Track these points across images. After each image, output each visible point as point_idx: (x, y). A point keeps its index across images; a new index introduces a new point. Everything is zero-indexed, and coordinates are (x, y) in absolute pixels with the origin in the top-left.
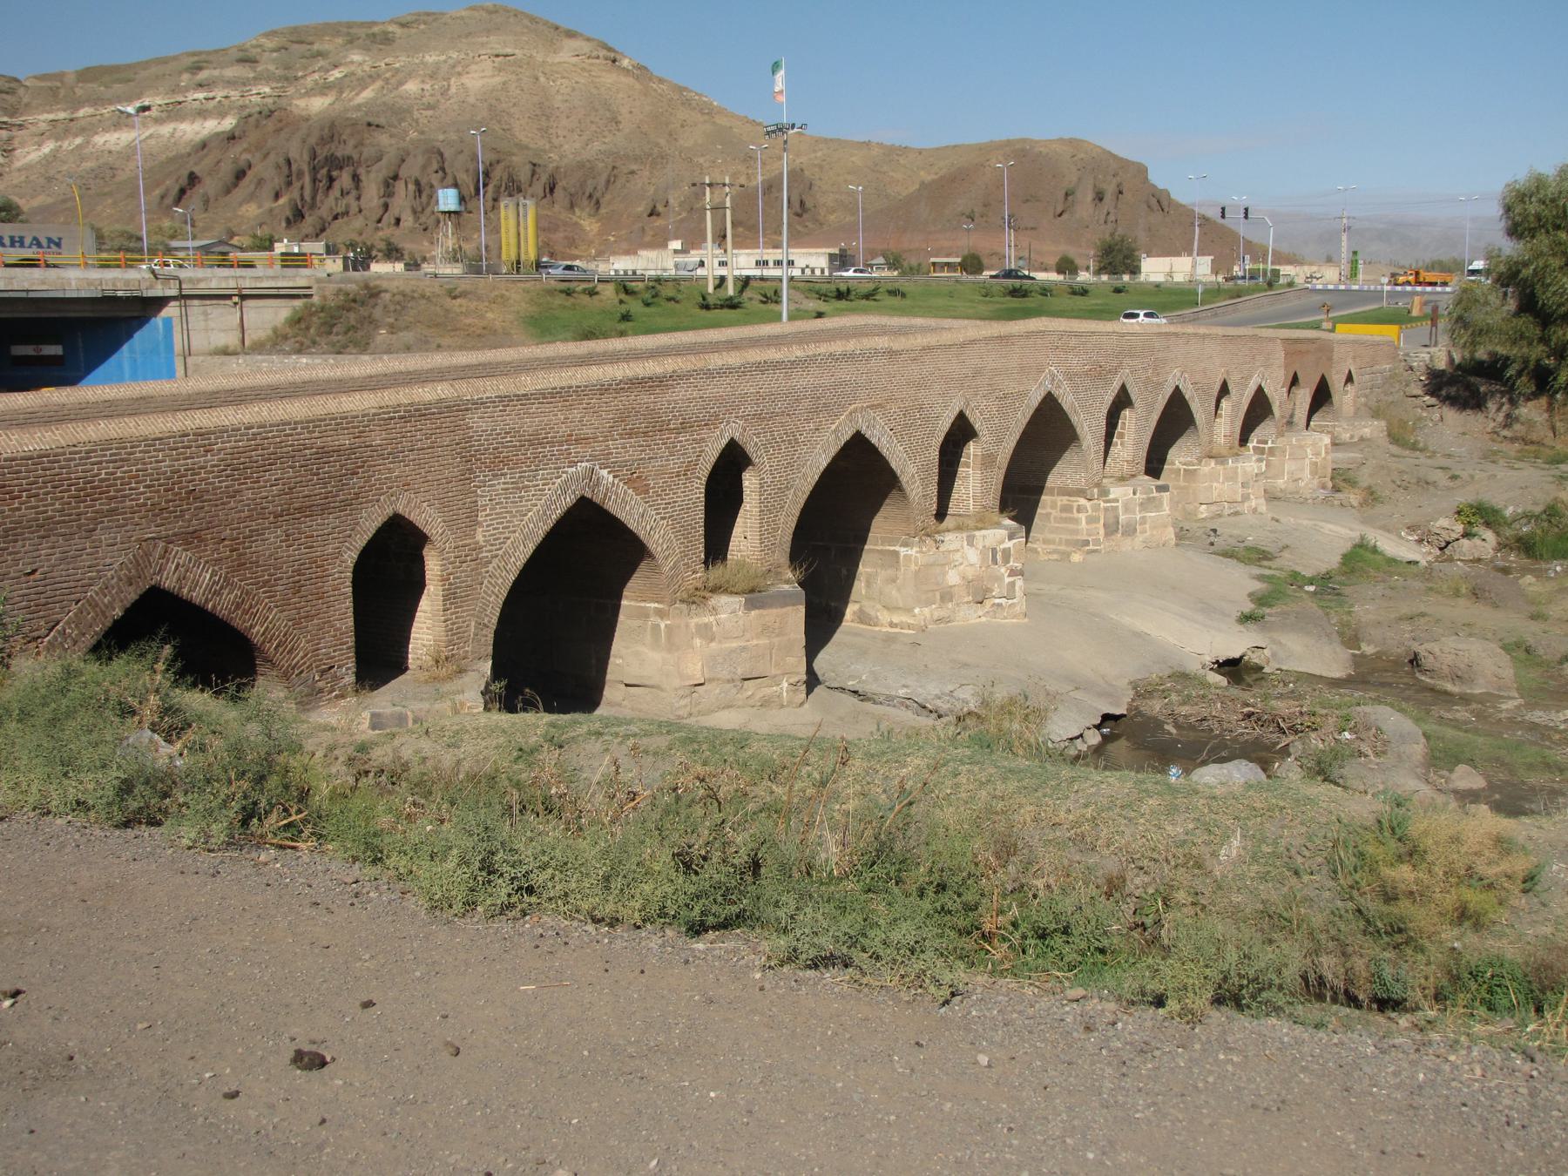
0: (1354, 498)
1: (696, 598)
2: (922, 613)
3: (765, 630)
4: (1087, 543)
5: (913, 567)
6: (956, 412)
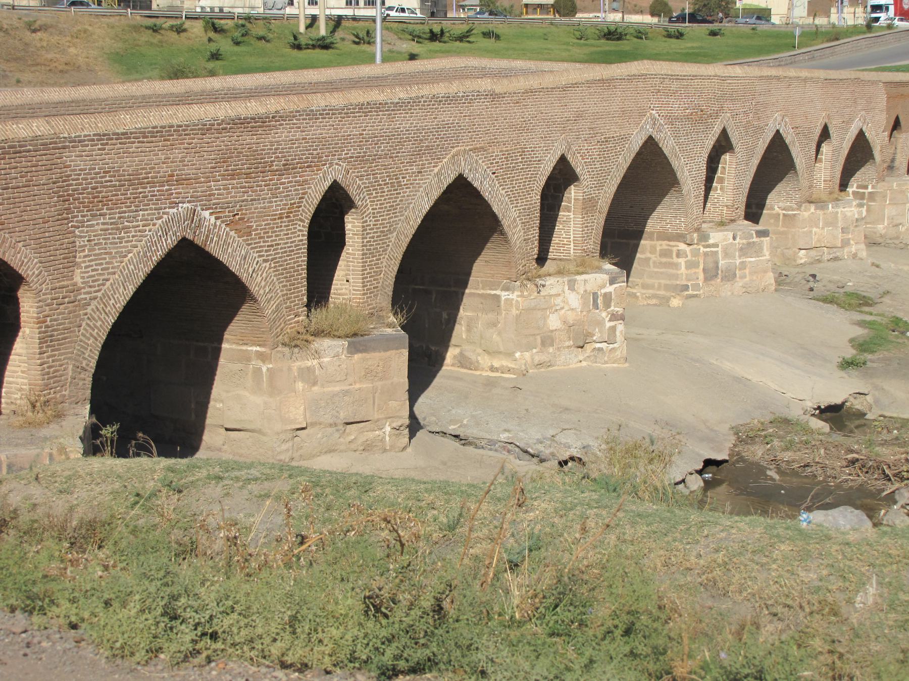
1: (297, 342)
2: (523, 357)
3: (369, 374)
4: (686, 288)
5: (514, 312)
6: (557, 157)
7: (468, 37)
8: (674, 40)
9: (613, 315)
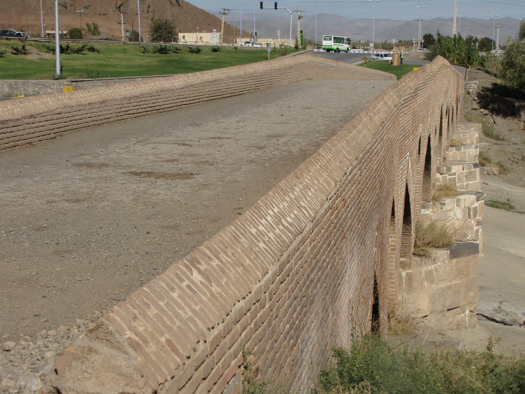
0: (496, 170)
3: (460, 273)
7: (82, 51)
8: (195, 54)
9: (478, 221)
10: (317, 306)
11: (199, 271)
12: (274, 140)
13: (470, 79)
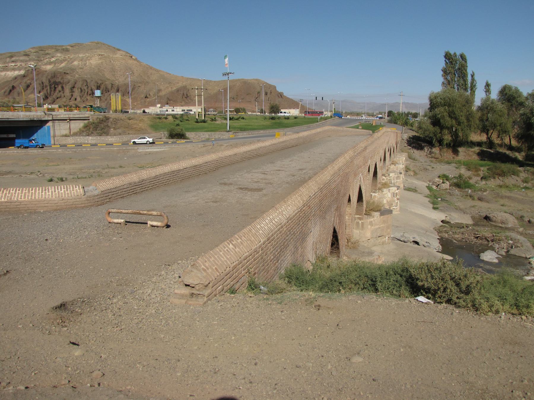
0: (412, 174)
3: (384, 222)
10: (291, 247)
11: (232, 244)
12: (300, 172)
13: (405, 133)
